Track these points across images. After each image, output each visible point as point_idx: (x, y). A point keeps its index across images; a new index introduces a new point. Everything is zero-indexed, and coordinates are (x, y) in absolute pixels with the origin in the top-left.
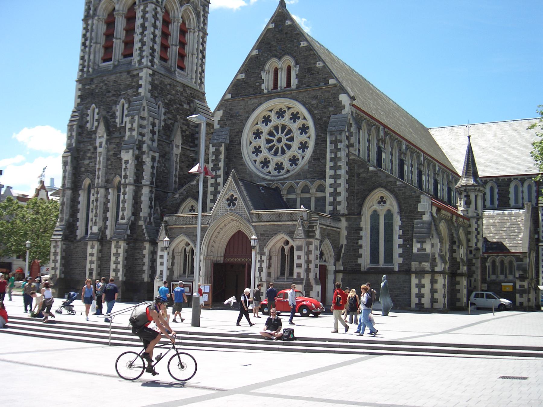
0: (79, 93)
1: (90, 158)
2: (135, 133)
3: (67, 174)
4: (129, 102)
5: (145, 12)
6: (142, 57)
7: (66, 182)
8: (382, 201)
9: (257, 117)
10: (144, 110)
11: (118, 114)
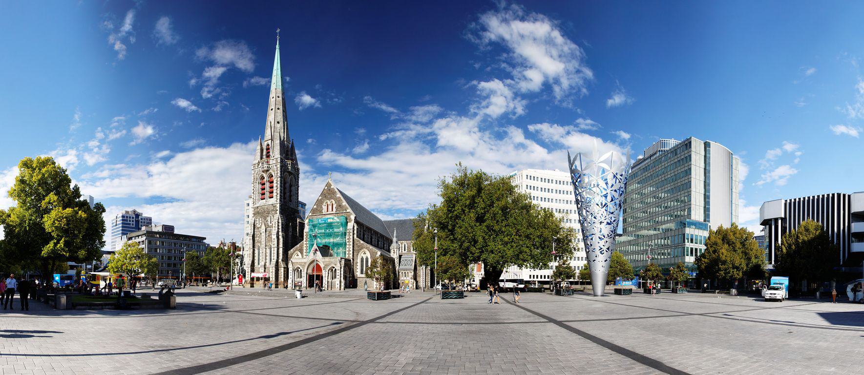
2: (277, 228)
4: (273, 216)
5: (277, 181)
6: (277, 199)
8: (365, 253)
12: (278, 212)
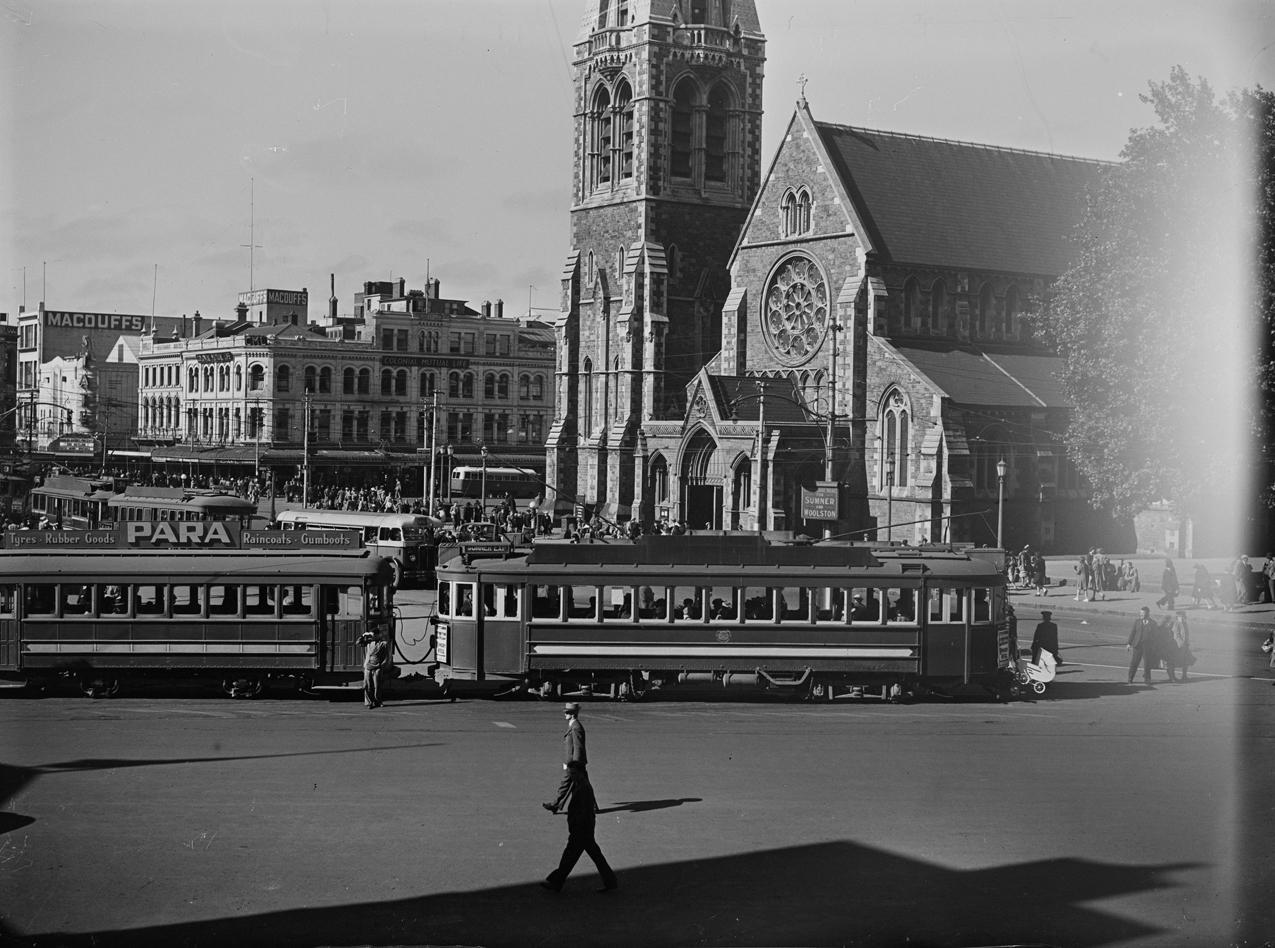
0: (575, 229)
10: (643, 263)
12: (642, 232)
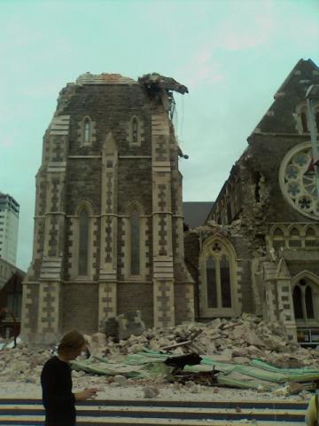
1: (86, 180)
2: (166, 155)
3: (59, 195)
7: (58, 204)
9: (292, 158)
11: (129, 131)
